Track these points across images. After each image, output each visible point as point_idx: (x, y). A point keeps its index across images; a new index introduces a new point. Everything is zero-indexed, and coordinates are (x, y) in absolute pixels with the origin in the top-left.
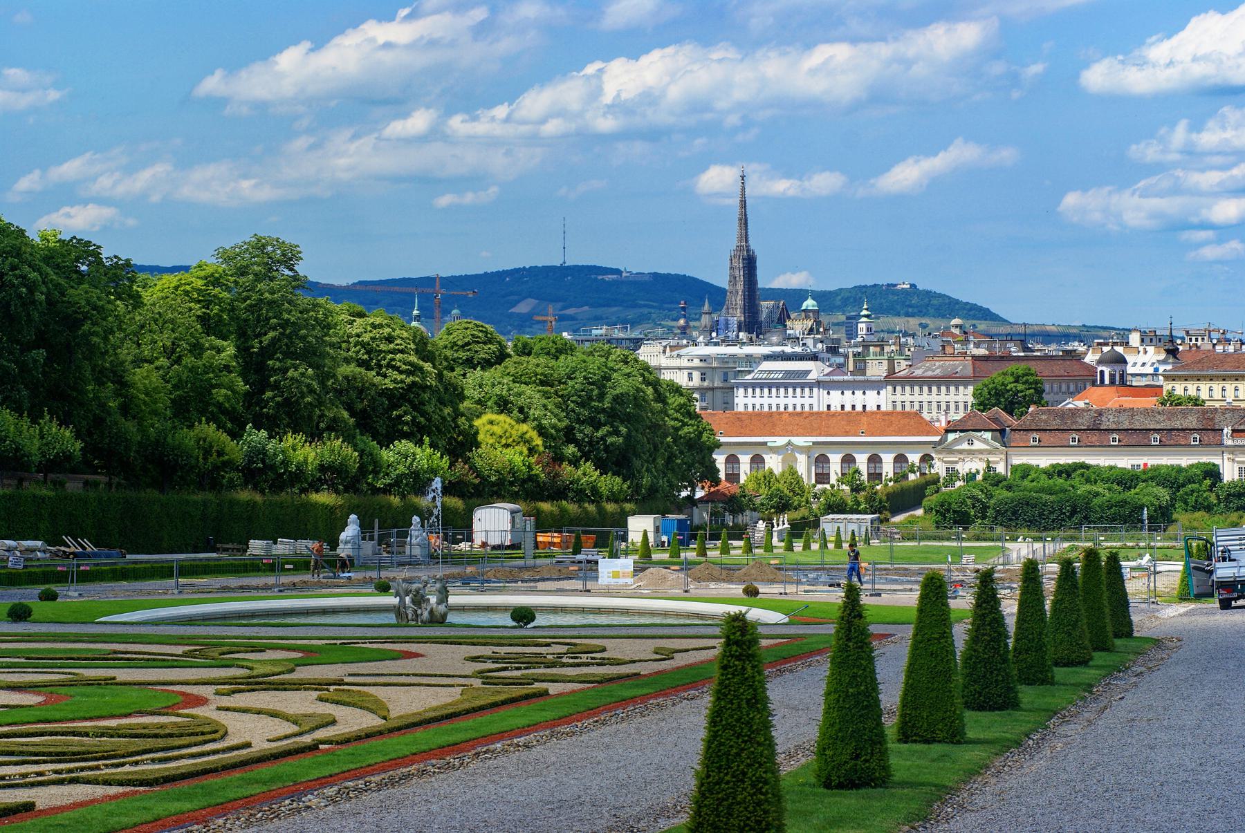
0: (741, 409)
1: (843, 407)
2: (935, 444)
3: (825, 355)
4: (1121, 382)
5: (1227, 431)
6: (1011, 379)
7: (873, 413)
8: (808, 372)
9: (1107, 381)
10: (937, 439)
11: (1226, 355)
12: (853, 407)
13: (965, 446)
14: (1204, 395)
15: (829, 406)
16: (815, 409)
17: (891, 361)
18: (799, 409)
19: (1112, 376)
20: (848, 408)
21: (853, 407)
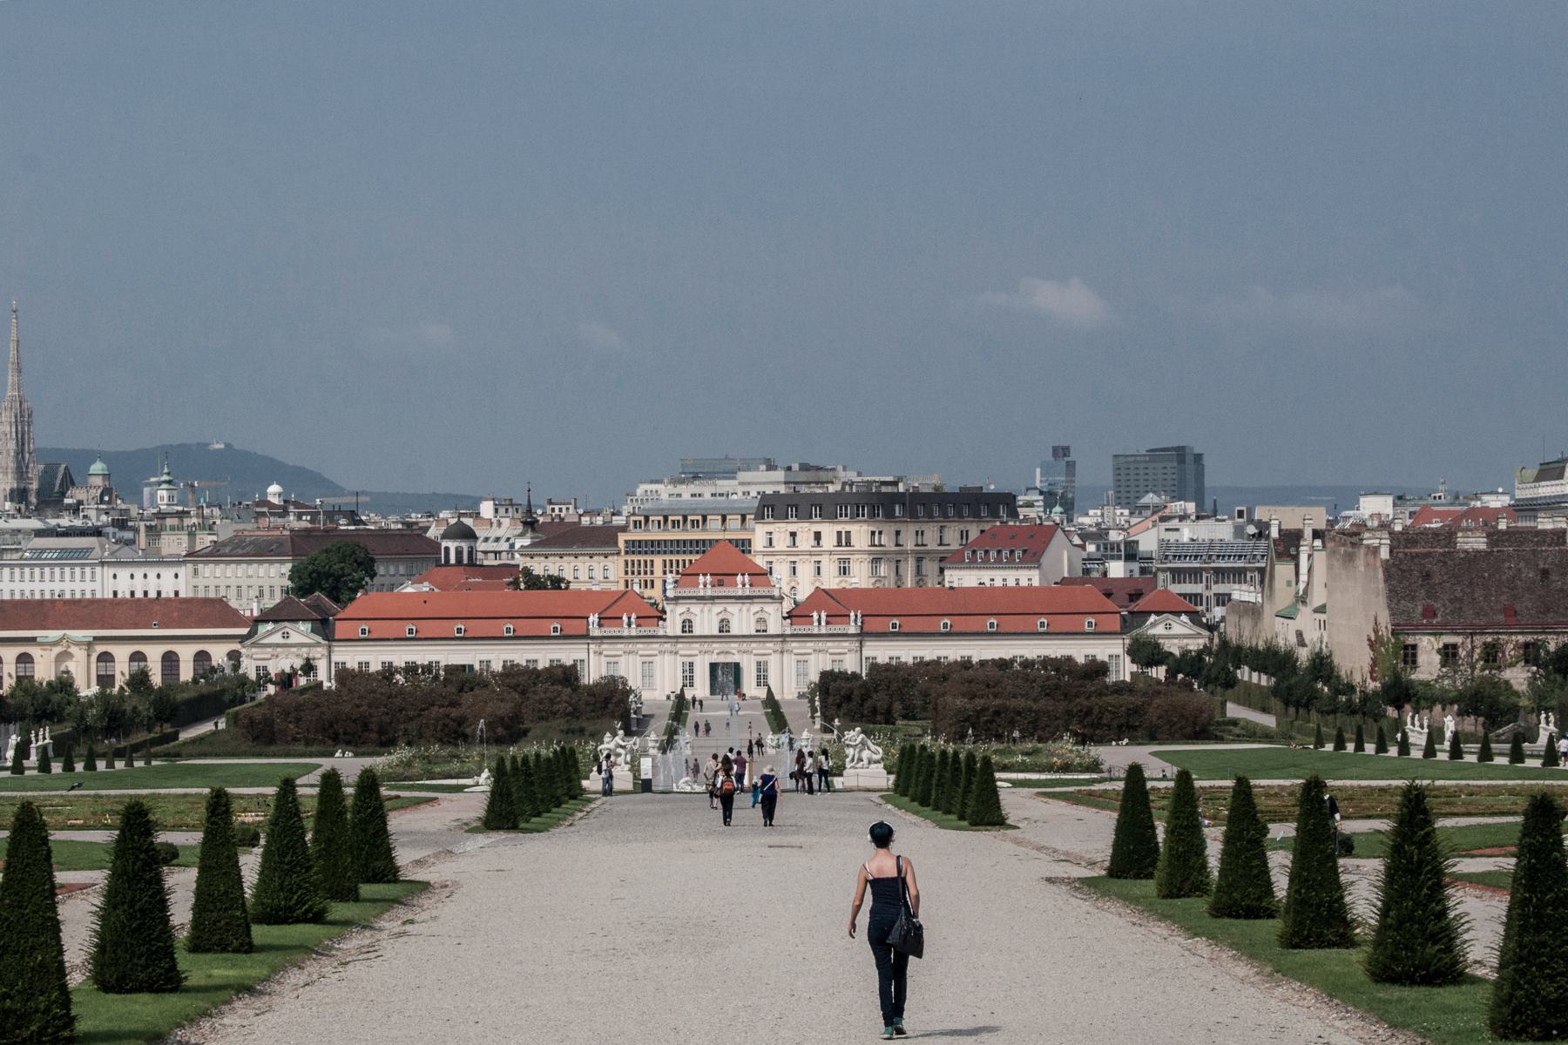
1: (132, 593)
2: (242, 639)
3: (110, 530)
4: (471, 564)
5: (593, 618)
6: (335, 558)
7: (168, 600)
8: (90, 550)
9: (453, 560)
10: (244, 631)
12: (146, 593)
13: (277, 638)
14: (568, 575)
15: (115, 593)
16: (99, 596)
17: (192, 535)
18: (78, 596)
19: (459, 552)
20: (139, 595)
21: (146, 593)
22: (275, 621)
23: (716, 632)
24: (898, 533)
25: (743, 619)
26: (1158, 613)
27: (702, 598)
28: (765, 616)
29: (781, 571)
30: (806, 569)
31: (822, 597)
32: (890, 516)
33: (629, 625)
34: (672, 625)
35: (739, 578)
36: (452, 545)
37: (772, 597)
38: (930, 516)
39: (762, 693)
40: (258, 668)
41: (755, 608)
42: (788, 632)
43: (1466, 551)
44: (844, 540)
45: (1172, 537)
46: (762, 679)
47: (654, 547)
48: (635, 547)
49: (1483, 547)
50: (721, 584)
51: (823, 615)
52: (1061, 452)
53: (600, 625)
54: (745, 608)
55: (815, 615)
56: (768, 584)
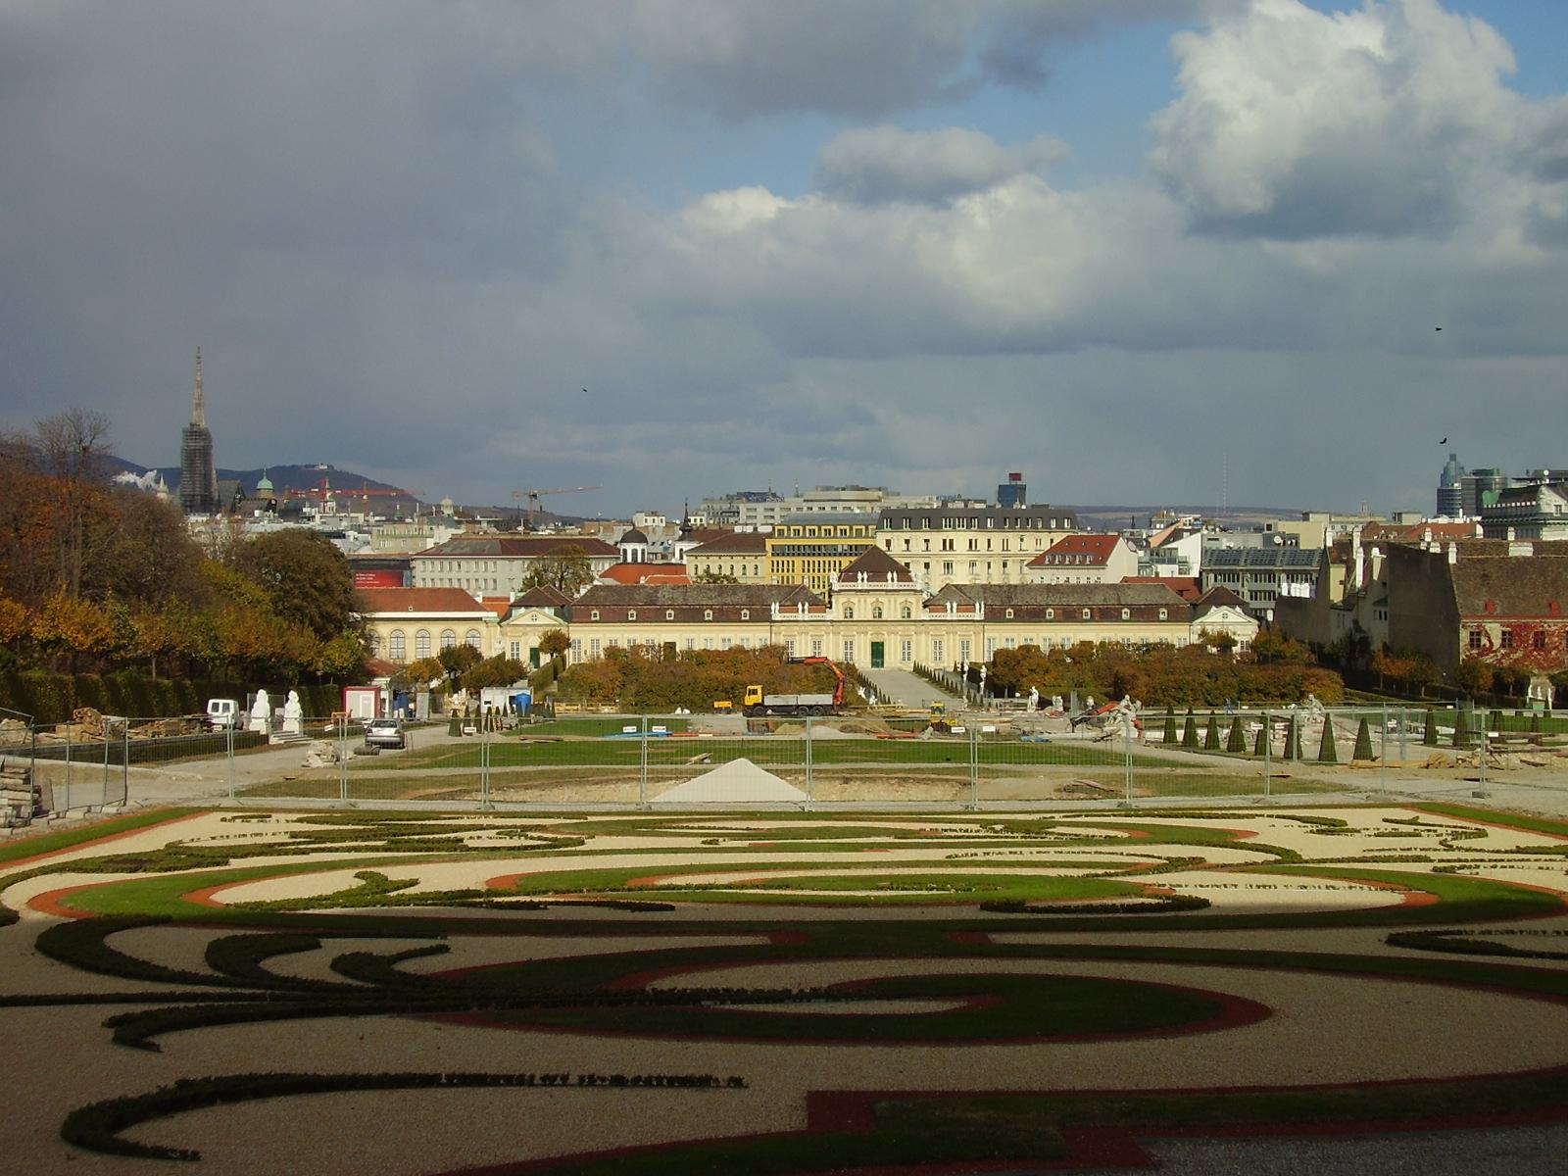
0: (419, 584)
3: (352, 534)
5: (775, 607)
9: (629, 560)
11: (743, 535)
19: (635, 552)
22: (526, 606)
24: (989, 541)
25: (892, 609)
26: (1218, 605)
27: (860, 591)
28: (909, 605)
29: (917, 570)
30: (937, 568)
31: (948, 590)
32: (982, 527)
33: (803, 611)
34: (836, 613)
35: (889, 575)
36: (629, 547)
38: (1012, 528)
40: (629, 641)
41: (901, 598)
43: (1516, 558)
44: (948, 545)
45: (1213, 545)
46: (906, 655)
47: (816, 550)
48: (778, 551)
49: (1531, 554)
51: (955, 605)
52: (1016, 477)
54: (892, 598)
55: (948, 605)
56: (910, 580)
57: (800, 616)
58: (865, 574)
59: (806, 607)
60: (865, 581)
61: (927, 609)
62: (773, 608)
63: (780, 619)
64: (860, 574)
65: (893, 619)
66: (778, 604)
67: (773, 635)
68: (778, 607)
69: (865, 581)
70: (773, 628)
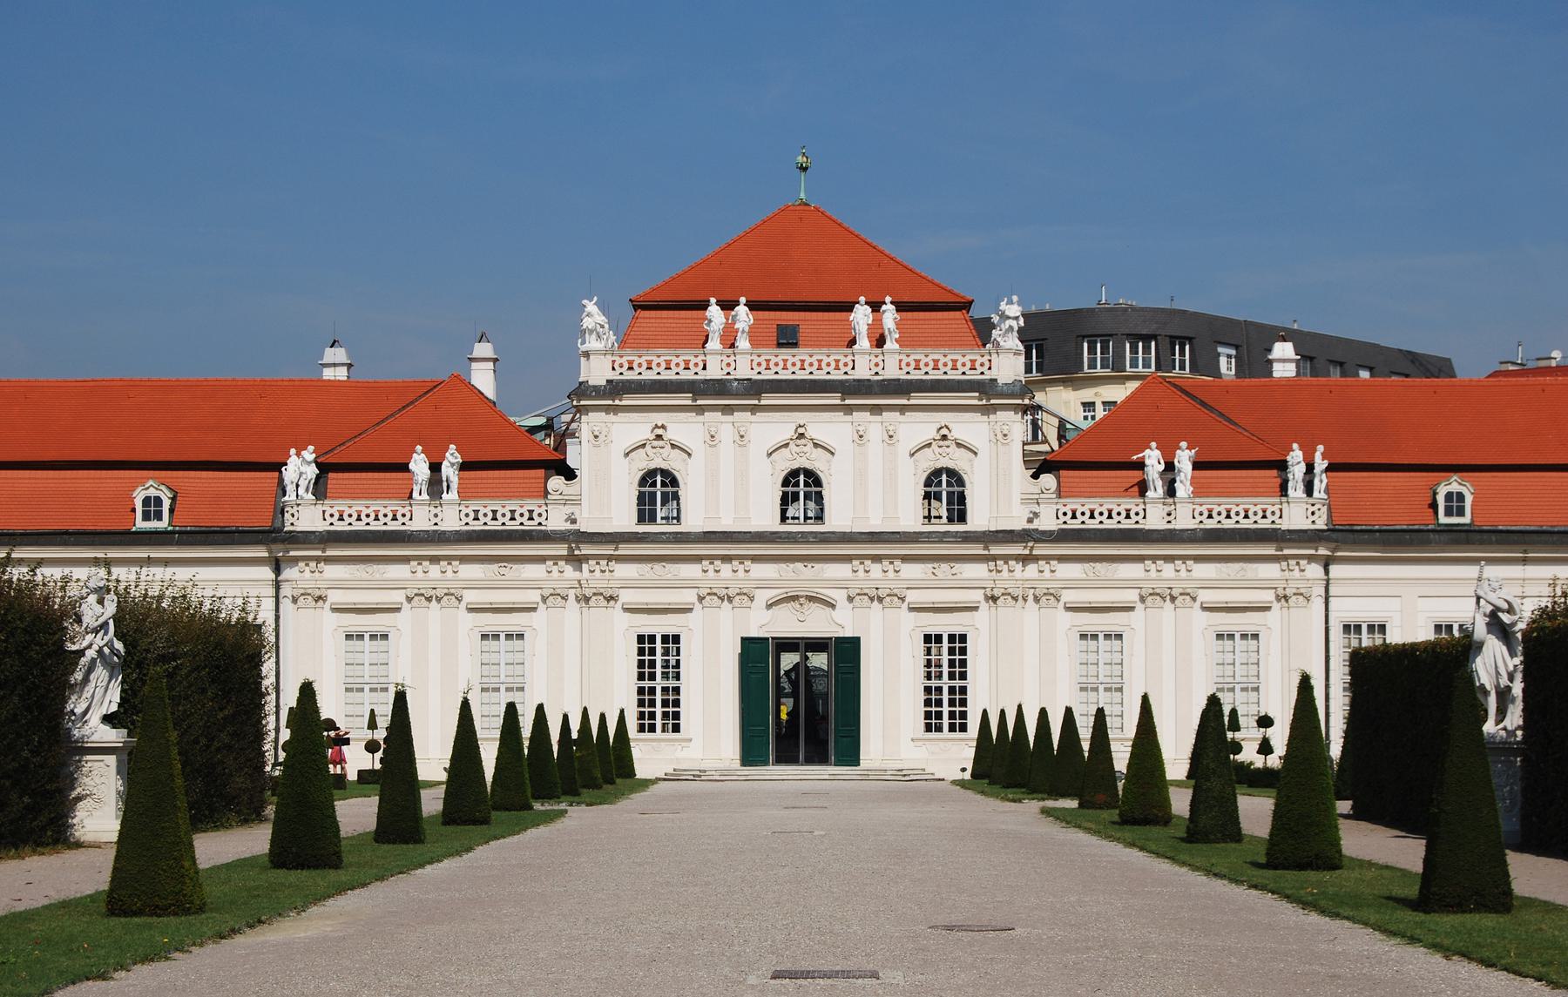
5: (300, 468)
23: (766, 518)
25: (873, 471)
27: (718, 388)
33: (436, 486)
34: (602, 491)
35: (861, 316)
37: (986, 388)
39: (955, 755)
41: (916, 428)
42: (1047, 522)
46: (943, 707)
50: (787, 339)
51: (1184, 459)
53: (320, 490)
55: (1153, 459)
57: (421, 519)
58: (742, 310)
59: (449, 471)
60: (743, 343)
61: (1048, 480)
62: (290, 473)
63: (321, 526)
64: (714, 311)
65: (876, 524)
66: (309, 455)
67: (286, 605)
68: (312, 471)
69: (743, 343)
70: (288, 573)
